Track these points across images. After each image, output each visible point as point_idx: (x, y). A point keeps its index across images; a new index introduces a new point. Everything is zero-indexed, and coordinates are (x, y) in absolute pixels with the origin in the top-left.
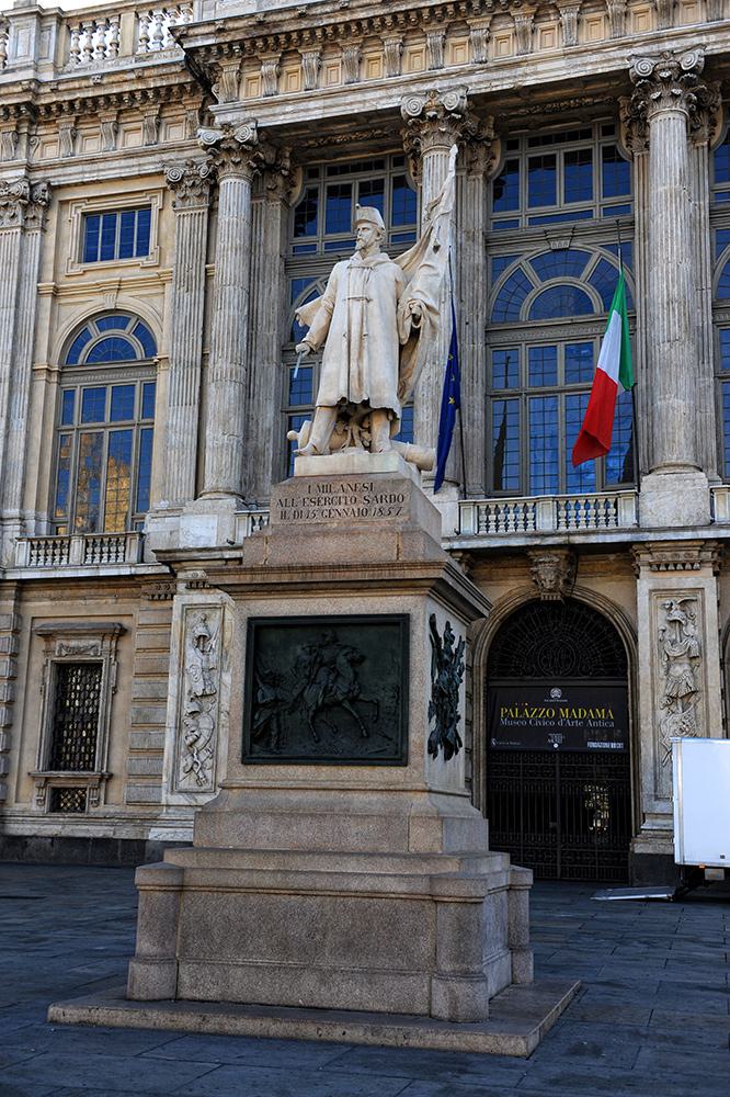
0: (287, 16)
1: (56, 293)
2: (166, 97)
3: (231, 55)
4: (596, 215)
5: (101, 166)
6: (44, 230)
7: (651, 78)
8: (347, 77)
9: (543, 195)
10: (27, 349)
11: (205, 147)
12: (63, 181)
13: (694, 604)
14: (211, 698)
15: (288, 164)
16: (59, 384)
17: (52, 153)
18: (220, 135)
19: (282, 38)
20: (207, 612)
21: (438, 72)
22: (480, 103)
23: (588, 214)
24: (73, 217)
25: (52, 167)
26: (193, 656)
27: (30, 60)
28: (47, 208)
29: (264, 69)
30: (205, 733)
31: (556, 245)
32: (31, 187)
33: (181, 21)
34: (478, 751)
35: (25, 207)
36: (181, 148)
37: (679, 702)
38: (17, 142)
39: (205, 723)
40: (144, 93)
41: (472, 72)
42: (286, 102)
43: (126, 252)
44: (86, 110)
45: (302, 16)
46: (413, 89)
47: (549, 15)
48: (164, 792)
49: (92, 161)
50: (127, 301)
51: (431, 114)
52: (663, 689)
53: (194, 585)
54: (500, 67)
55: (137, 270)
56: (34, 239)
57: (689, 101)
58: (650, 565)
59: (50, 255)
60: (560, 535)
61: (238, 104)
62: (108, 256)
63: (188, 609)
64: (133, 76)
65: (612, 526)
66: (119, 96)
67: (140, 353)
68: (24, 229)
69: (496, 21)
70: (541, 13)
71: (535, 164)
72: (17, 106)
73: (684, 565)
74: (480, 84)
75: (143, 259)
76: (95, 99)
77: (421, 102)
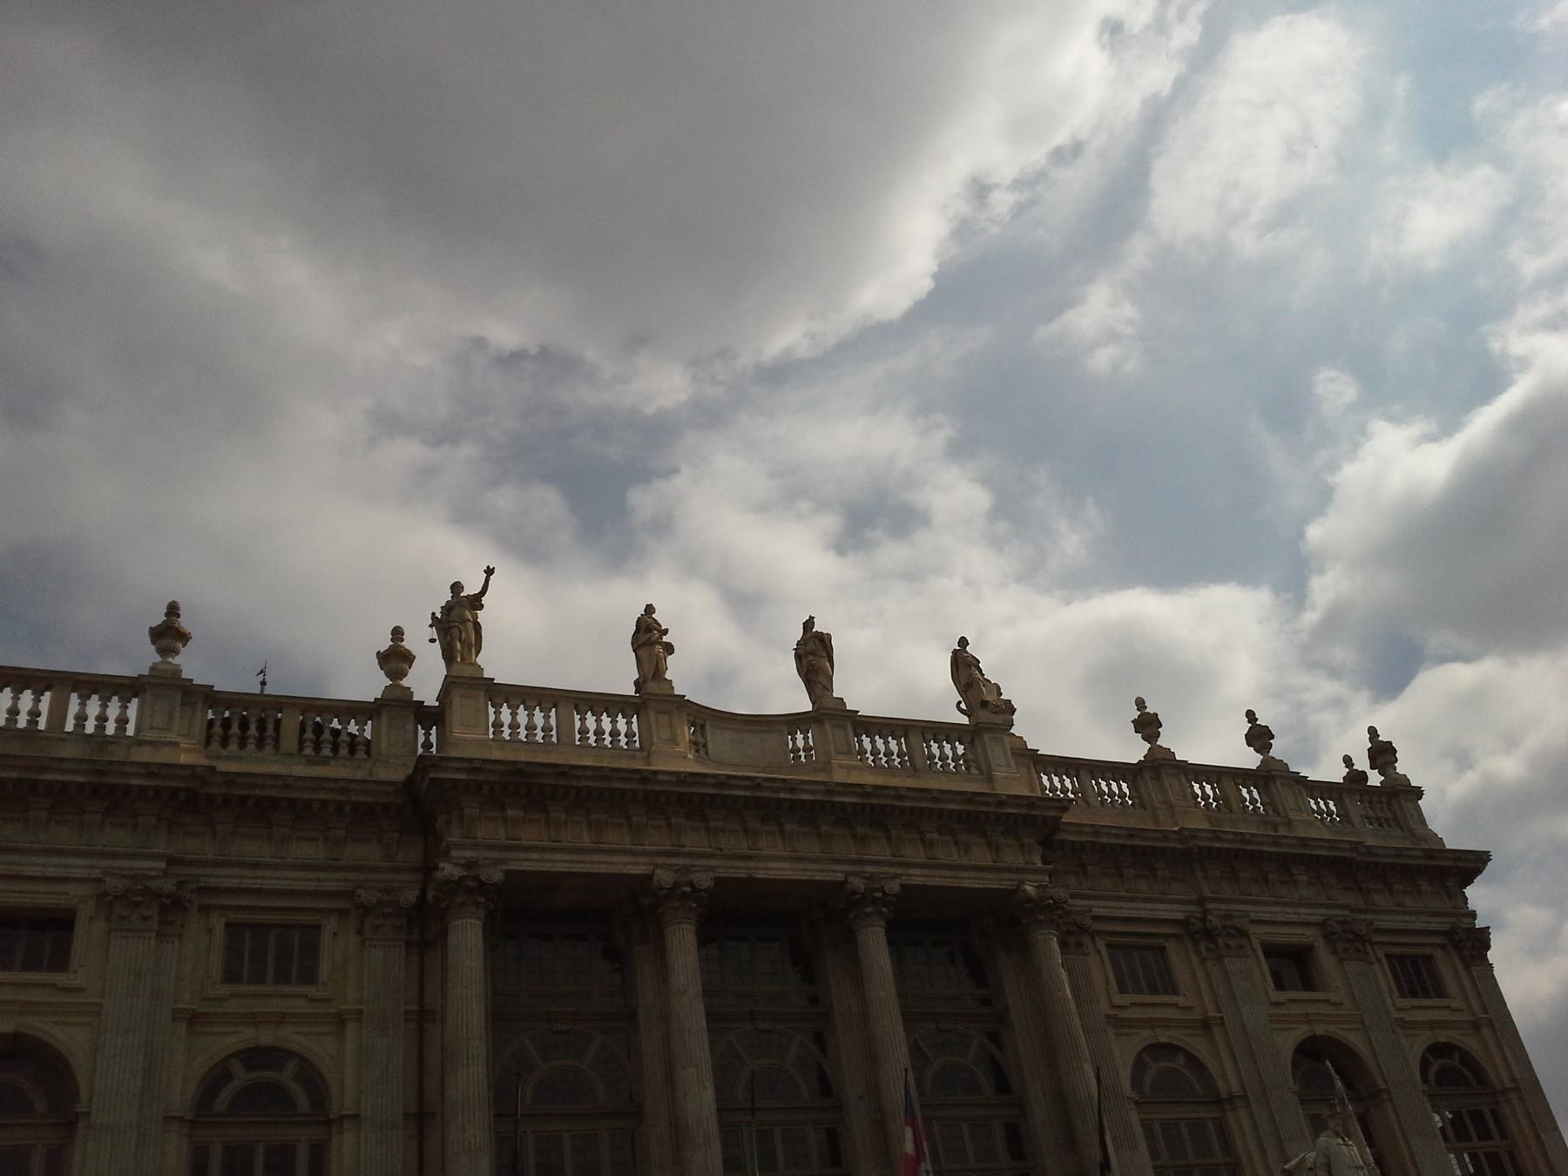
12: (213, 882)
24: (218, 923)
32: (180, 884)
36: (374, 869)
41: (711, 856)
43: (283, 977)
46: (659, 861)
49: (256, 866)
50: (290, 1037)
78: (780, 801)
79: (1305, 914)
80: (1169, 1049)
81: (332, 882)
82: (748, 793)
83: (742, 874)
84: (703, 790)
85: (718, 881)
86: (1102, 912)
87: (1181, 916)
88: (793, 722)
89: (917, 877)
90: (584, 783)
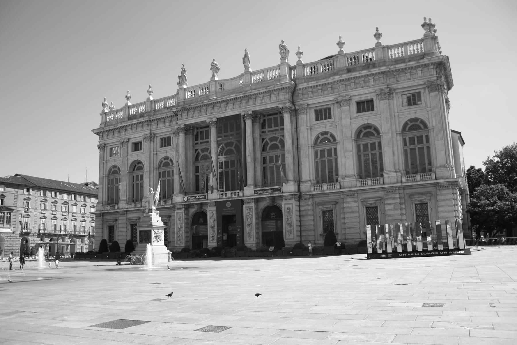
1: (156, 154)
2: (171, 117)
6: (154, 142)
10: (152, 165)
17: (154, 127)
18: (178, 126)
22: (218, 119)
26: (178, 222)
28: (154, 137)
32: (151, 134)
39: (181, 232)
43: (168, 146)
50: (168, 155)
52: (247, 223)
53: (178, 209)
59: (155, 147)
62: (165, 146)
63: (177, 213)
67: (171, 164)
79: (371, 90)
80: (326, 133)
85: (217, 119)
86: (312, 103)
87: (333, 99)
88: (240, 77)
89: (258, 108)
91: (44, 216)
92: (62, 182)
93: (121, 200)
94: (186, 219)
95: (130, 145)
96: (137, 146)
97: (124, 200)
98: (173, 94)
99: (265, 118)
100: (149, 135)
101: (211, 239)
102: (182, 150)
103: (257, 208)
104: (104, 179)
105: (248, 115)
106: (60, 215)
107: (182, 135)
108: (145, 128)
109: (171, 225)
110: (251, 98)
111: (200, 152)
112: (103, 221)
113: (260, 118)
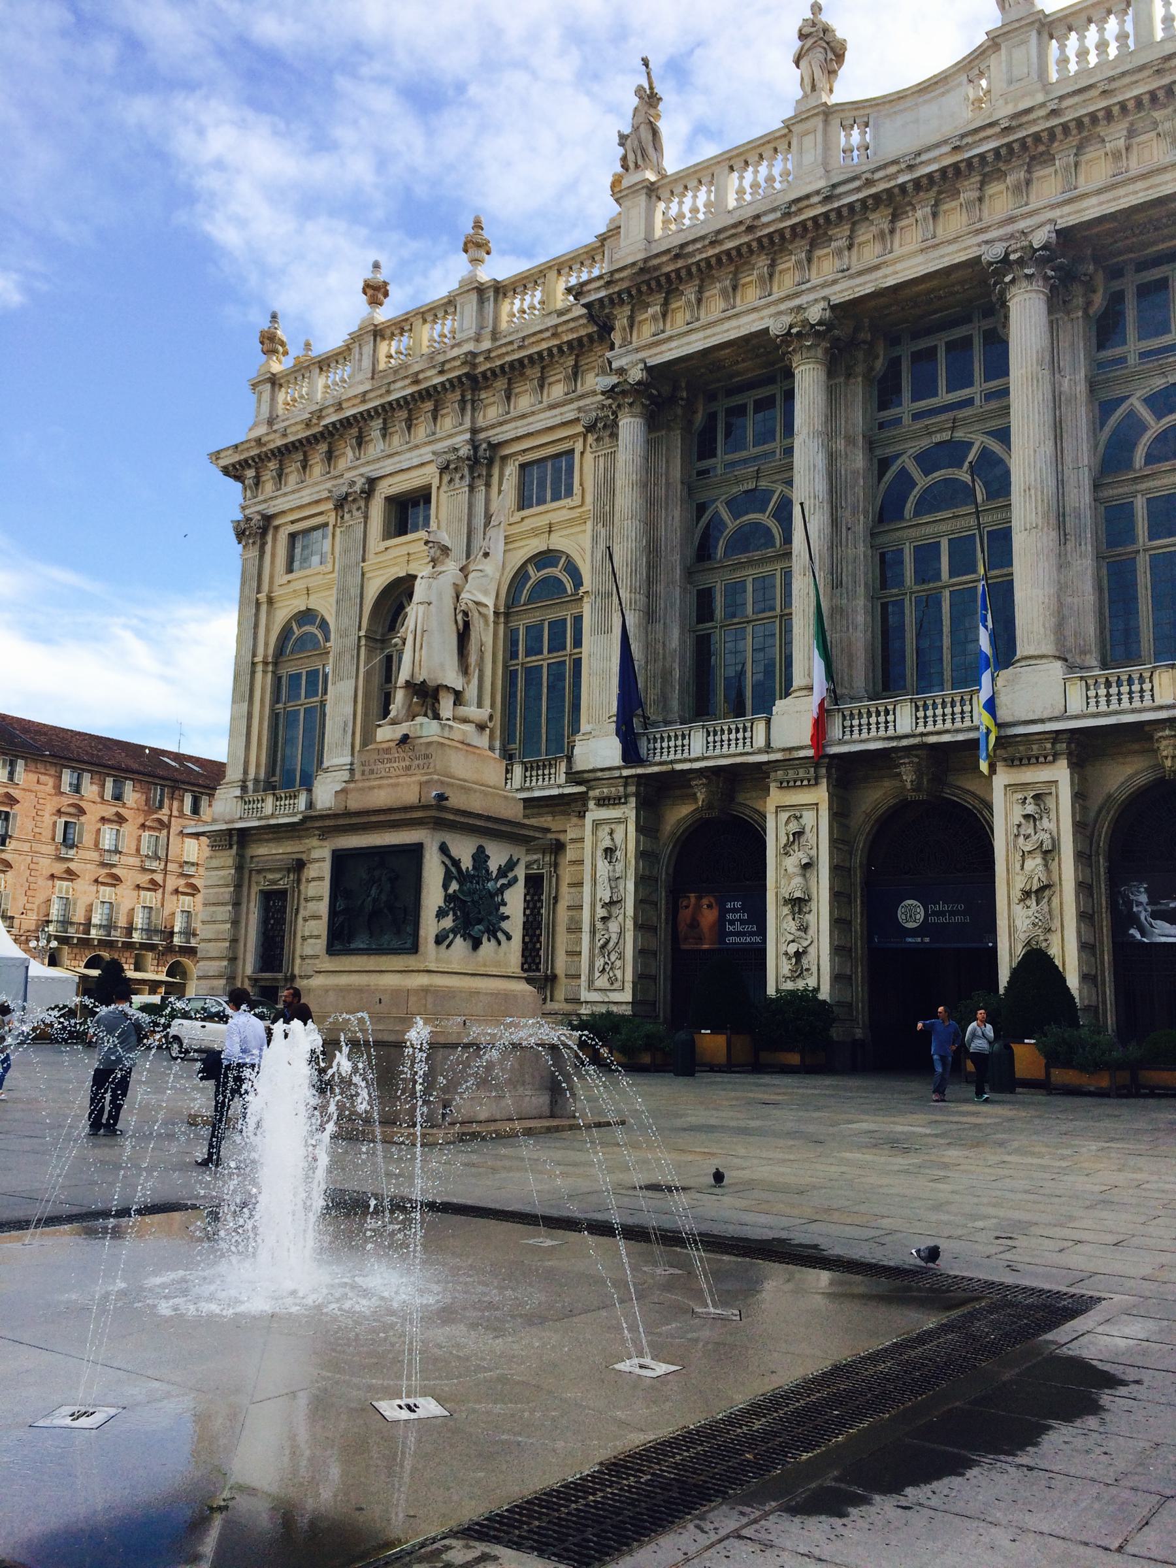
0: (664, 259)
2: (579, 347)
3: (622, 302)
4: (977, 402)
5: (530, 419)
6: (488, 485)
7: (1005, 260)
8: (722, 305)
9: (924, 389)
11: (603, 393)
13: (1049, 797)
14: (619, 905)
15: (685, 394)
16: (506, 623)
17: (492, 413)
18: (614, 379)
19: (663, 280)
20: (613, 826)
21: (804, 287)
22: (842, 311)
23: (969, 402)
25: (493, 426)
26: (603, 867)
27: (471, 333)
29: (651, 311)
30: (614, 937)
31: (938, 438)
32: (476, 448)
33: (573, 281)
34: (856, 949)
35: (472, 469)
37: (1033, 896)
38: (463, 410)
39: (614, 926)
40: (559, 347)
41: (834, 282)
42: (670, 338)
43: (556, 497)
44: (514, 372)
45: (677, 257)
46: (783, 307)
47: (907, 212)
48: (582, 988)
49: (523, 416)
50: (558, 542)
51: (794, 331)
52: (1019, 883)
53: (602, 802)
54: (860, 273)
55: (565, 511)
56: (480, 496)
57: (1046, 278)
58: (1005, 760)
60: (914, 736)
61: (630, 347)
62: (541, 501)
63: (597, 824)
64: (548, 334)
65: (1148, 702)
66: (540, 353)
68: (472, 488)
69: (858, 226)
70: (899, 211)
71: (917, 357)
72: (459, 378)
73: (1037, 758)
74: (843, 292)
75: (569, 500)
76: (520, 361)
77: (787, 320)
78: (902, 187)
81: (569, 412)
82: (860, 196)
83: (869, 289)
84: (811, 213)
89: (1092, 209)
90: (698, 258)
91: (69, 871)
92: (150, 749)
93: (326, 770)
94: (641, 855)
95: (377, 509)
96: (407, 511)
97: (339, 769)
98: (587, 238)
99: (1116, 285)
100: (465, 451)
101: (786, 967)
102: (627, 500)
103: (1079, 797)
104: (259, 675)
105: (1032, 255)
106: (130, 867)
107: (630, 427)
108: (448, 423)
109: (564, 889)
110: (1047, 159)
111: (725, 515)
112: (239, 868)
113: (1091, 289)
